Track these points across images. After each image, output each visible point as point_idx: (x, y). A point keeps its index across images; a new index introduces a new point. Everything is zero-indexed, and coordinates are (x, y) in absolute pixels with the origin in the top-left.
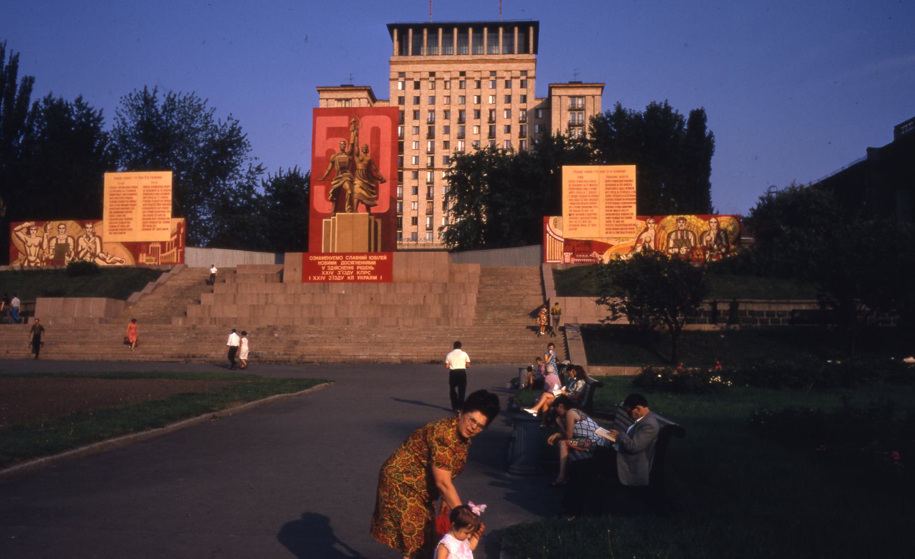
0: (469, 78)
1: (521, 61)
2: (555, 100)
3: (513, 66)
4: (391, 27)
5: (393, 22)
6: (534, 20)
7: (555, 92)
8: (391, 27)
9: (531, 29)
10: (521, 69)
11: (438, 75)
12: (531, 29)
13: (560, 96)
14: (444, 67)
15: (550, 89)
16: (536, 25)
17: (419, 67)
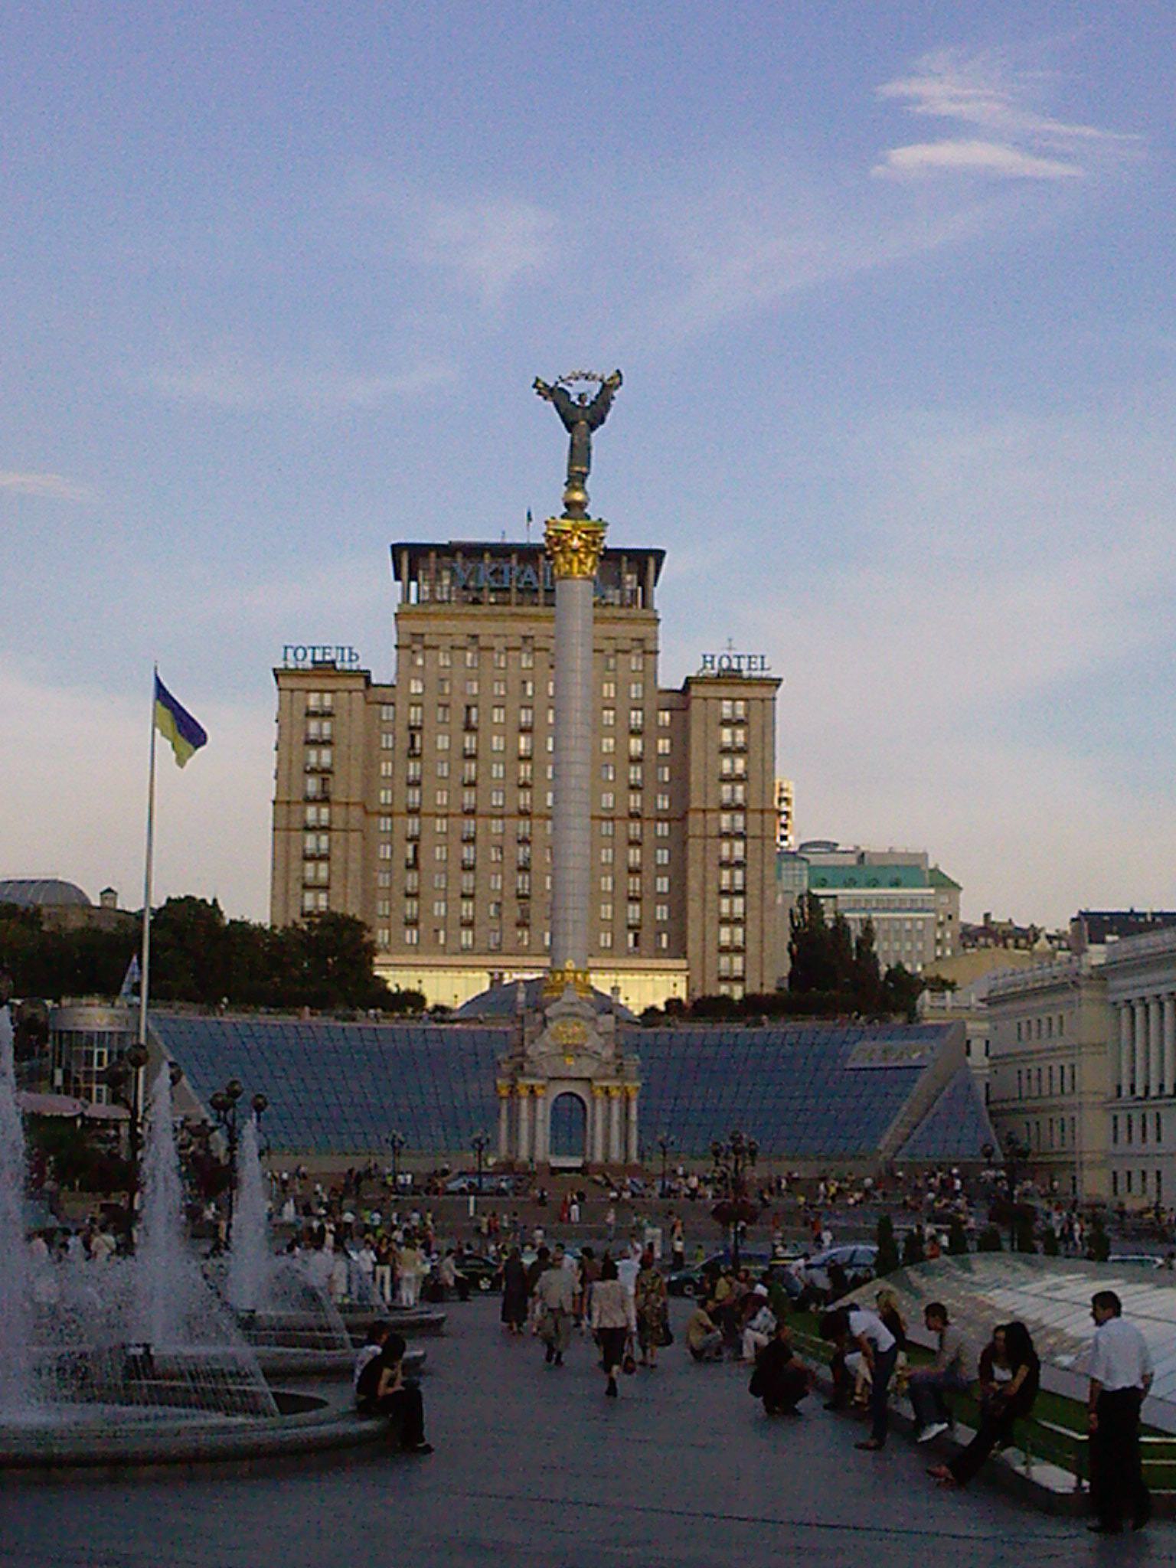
0: (540, 649)
1: (631, 620)
2: (696, 705)
3: (619, 630)
4: (397, 549)
5: (402, 540)
6: (655, 547)
7: (695, 690)
8: (397, 549)
9: (652, 562)
10: (634, 636)
11: (483, 641)
12: (652, 562)
13: (705, 699)
14: (494, 627)
15: (688, 681)
16: (659, 555)
17: (450, 626)
